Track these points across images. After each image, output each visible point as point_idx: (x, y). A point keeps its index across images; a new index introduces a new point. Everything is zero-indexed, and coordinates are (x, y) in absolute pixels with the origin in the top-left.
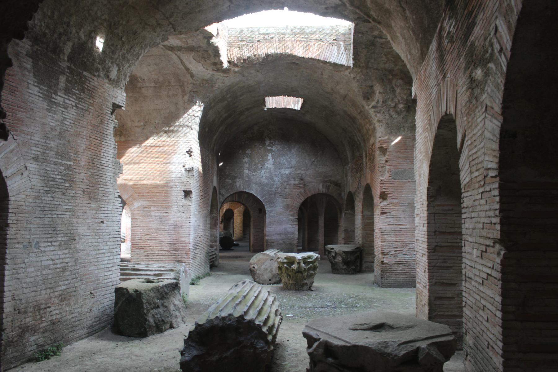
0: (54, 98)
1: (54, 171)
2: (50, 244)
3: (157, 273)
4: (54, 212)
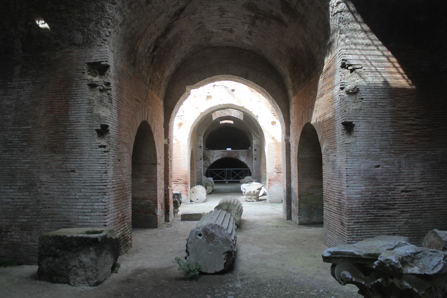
0: (9, 85)
1: (11, 136)
2: (9, 187)
4: (12, 165)
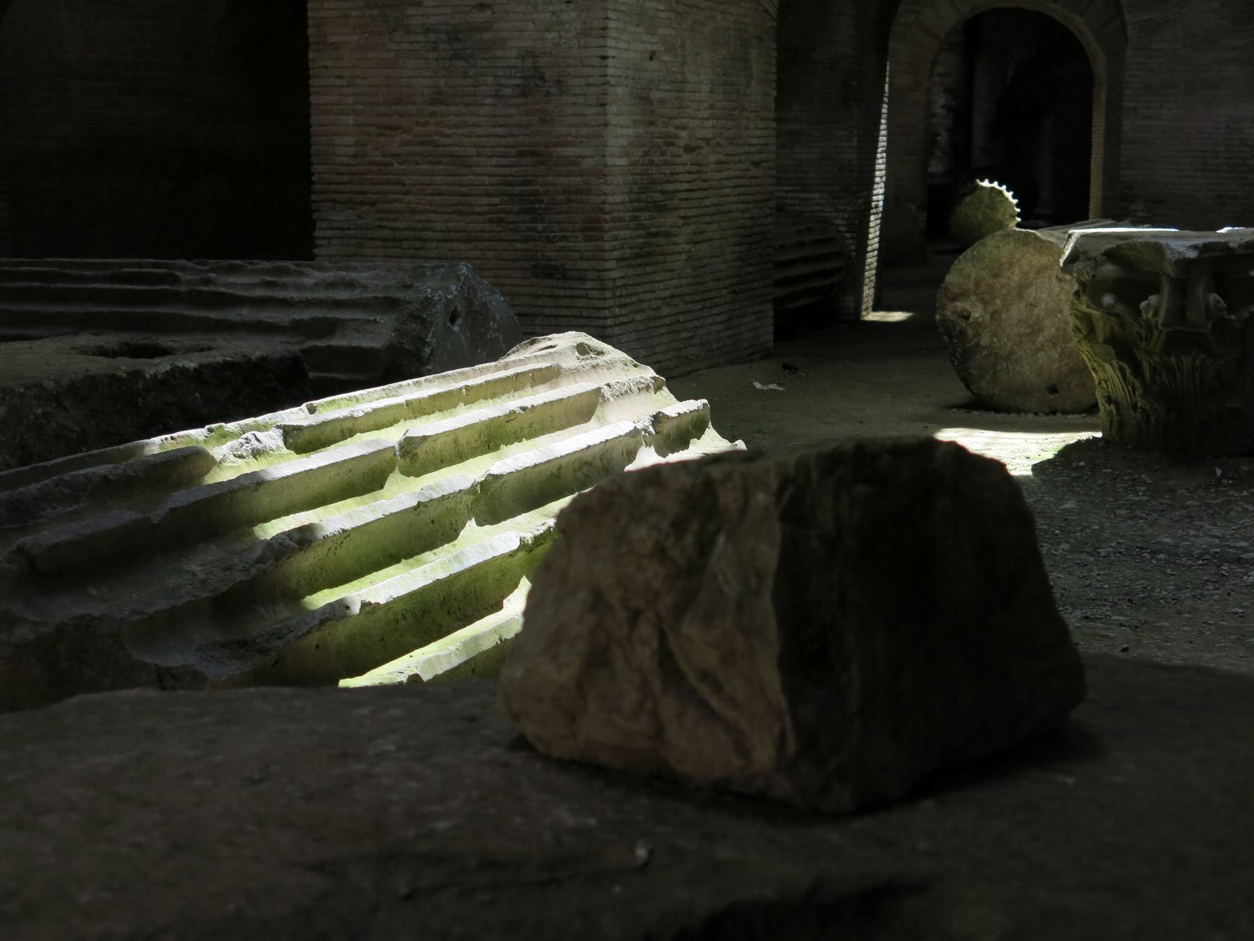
3: (306, 315)
